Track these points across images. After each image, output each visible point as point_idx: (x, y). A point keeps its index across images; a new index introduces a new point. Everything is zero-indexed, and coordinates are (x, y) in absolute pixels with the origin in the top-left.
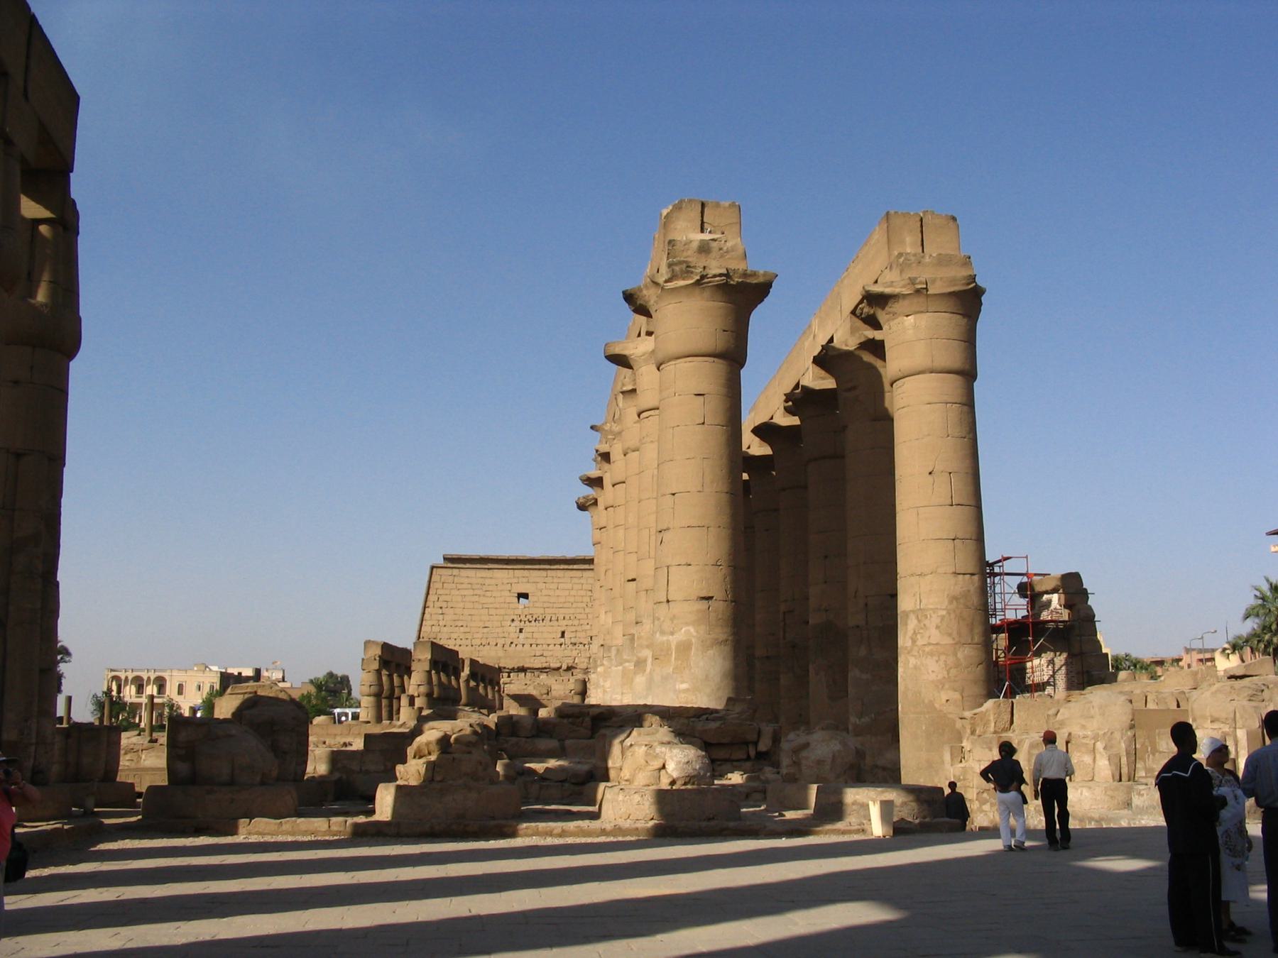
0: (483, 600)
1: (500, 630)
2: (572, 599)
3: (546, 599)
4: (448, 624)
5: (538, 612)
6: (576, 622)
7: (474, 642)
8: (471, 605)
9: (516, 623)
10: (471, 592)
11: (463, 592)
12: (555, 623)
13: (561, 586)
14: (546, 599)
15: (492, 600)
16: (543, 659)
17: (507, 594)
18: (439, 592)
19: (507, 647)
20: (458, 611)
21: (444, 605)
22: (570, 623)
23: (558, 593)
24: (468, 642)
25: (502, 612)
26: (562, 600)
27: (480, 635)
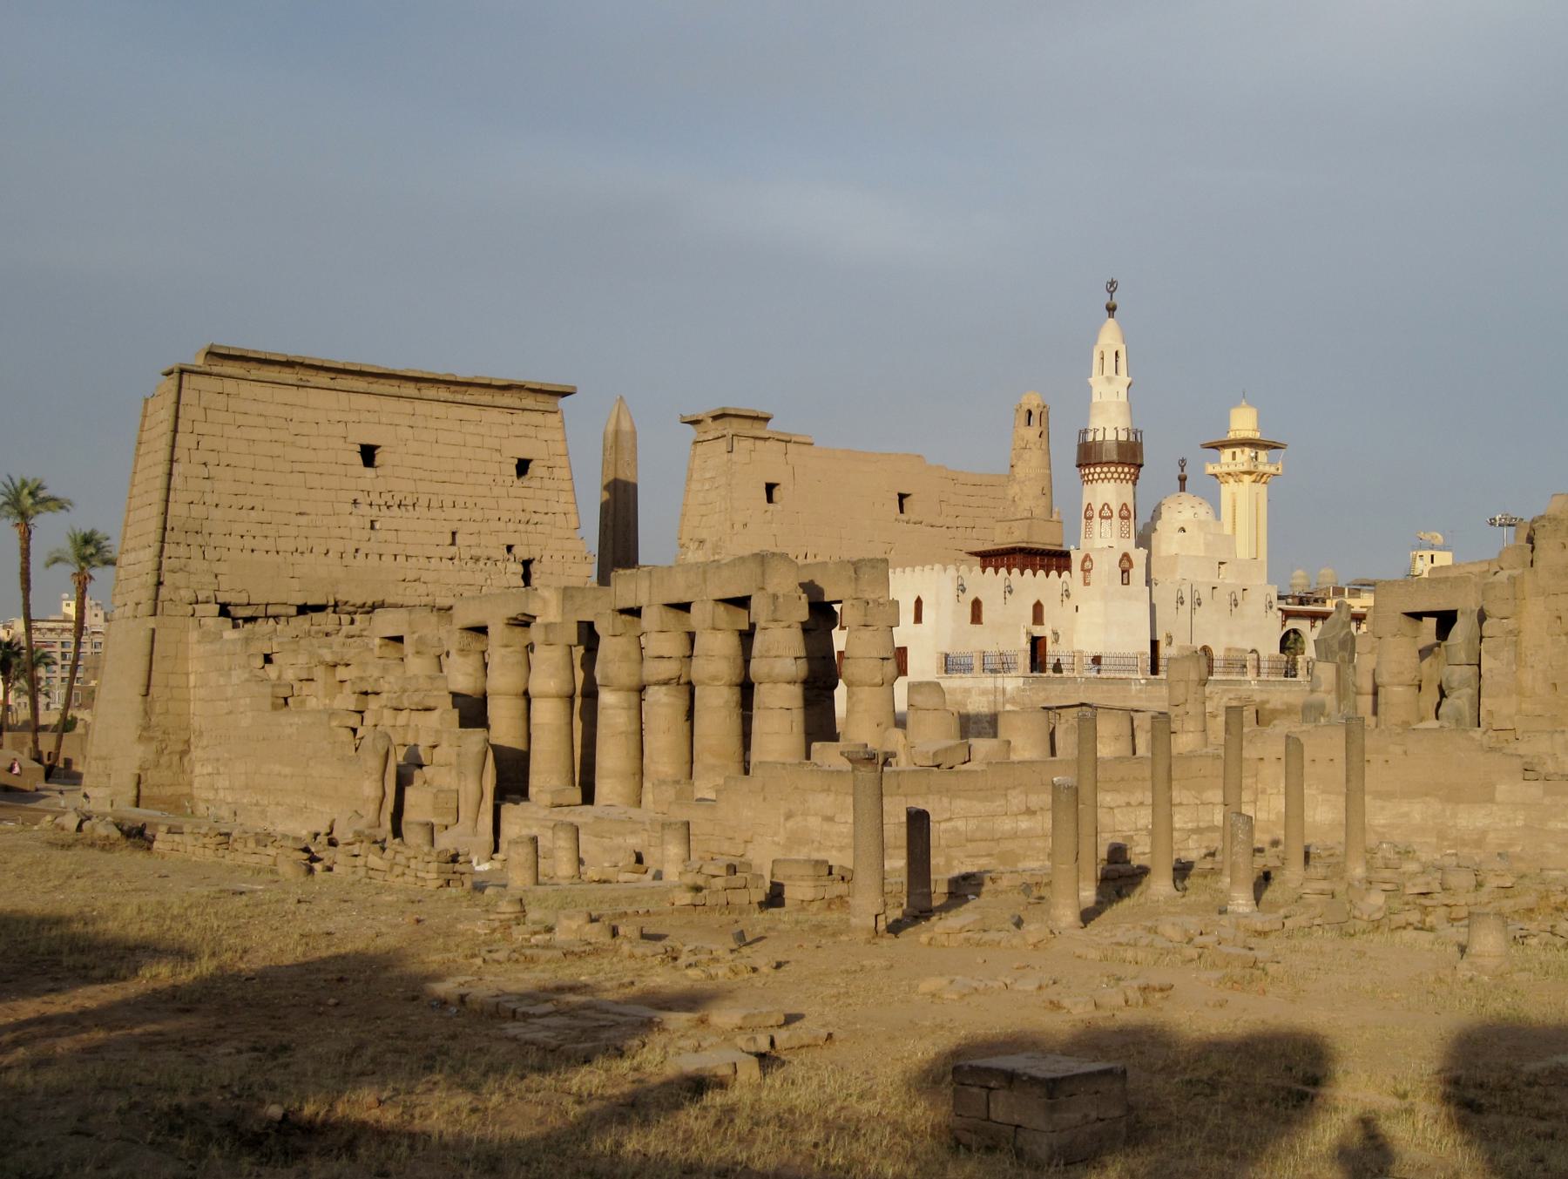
6: (477, 514)
7: (283, 545)
9: (363, 508)
12: (435, 513)
16: (422, 589)
17: (340, 444)
18: (199, 428)
19: (348, 558)
21: (212, 458)
22: (466, 514)
24: (269, 544)
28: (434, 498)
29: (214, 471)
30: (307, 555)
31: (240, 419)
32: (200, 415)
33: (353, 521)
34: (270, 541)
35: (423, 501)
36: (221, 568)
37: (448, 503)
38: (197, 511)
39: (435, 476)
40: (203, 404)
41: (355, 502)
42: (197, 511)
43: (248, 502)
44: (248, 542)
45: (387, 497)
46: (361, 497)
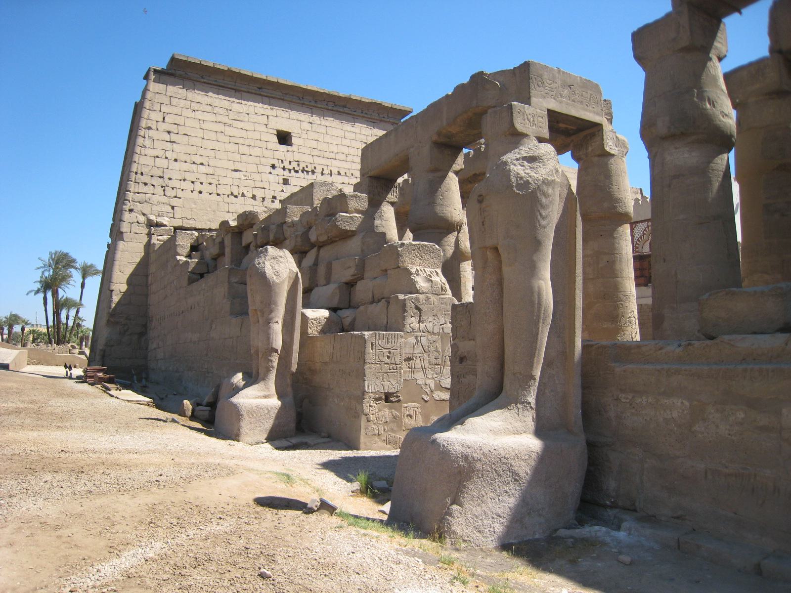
0: (229, 131)
1: (257, 177)
2: (346, 150)
3: (314, 144)
4: (183, 157)
5: (306, 160)
8: (213, 136)
10: (212, 117)
11: (199, 115)
13: (330, 131)
14: (314, 144)
15: (243, 134)
17: (263, 128)
18: (165, 109)
20: (193, 141)
21: (174, 128)
23: (328, 139)
24: (212, 189)
25: (256, 152)
26: (334, 149)
27: (230, 181)
28: (325, 168)
29: (174, 137)
30: (240, 197)
31: (195, 106)
32: (166, 100)
33: (271, 177)
34: (213, 186)
35: (319, 170)
36: (174, 202)
37: (335, 171)
38: (161, 162)
39: (326, 155)
40: (168, 94)
41: (273, 167)
42: (161, 162)
43: (199, 160)
44: (198, 187)
45: (294, 165)
46: (277, 163)
